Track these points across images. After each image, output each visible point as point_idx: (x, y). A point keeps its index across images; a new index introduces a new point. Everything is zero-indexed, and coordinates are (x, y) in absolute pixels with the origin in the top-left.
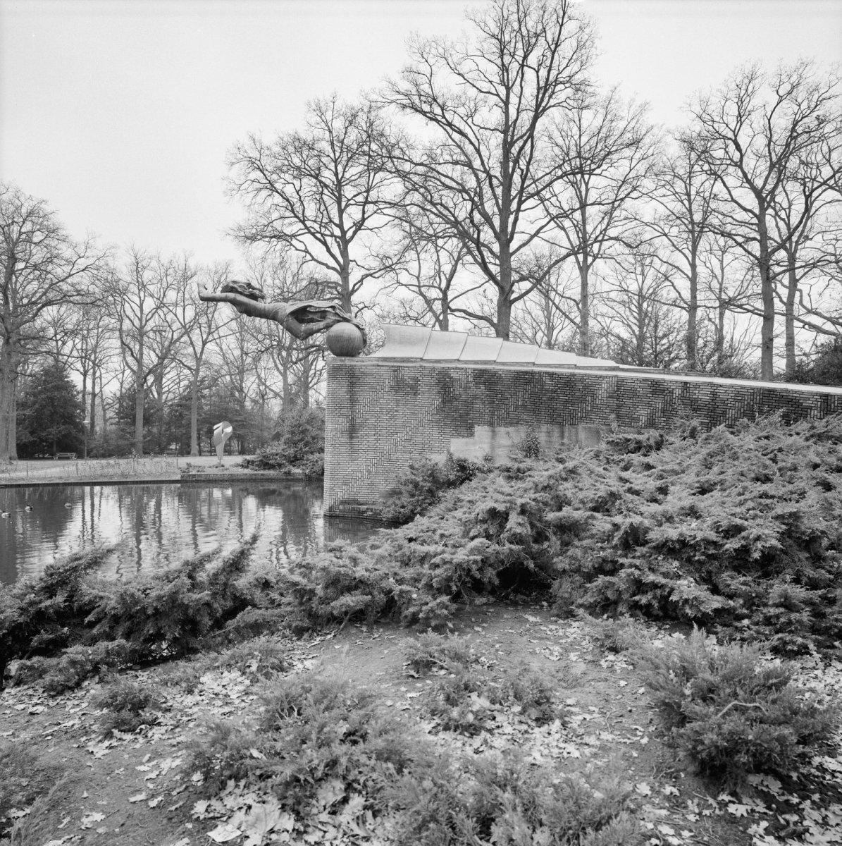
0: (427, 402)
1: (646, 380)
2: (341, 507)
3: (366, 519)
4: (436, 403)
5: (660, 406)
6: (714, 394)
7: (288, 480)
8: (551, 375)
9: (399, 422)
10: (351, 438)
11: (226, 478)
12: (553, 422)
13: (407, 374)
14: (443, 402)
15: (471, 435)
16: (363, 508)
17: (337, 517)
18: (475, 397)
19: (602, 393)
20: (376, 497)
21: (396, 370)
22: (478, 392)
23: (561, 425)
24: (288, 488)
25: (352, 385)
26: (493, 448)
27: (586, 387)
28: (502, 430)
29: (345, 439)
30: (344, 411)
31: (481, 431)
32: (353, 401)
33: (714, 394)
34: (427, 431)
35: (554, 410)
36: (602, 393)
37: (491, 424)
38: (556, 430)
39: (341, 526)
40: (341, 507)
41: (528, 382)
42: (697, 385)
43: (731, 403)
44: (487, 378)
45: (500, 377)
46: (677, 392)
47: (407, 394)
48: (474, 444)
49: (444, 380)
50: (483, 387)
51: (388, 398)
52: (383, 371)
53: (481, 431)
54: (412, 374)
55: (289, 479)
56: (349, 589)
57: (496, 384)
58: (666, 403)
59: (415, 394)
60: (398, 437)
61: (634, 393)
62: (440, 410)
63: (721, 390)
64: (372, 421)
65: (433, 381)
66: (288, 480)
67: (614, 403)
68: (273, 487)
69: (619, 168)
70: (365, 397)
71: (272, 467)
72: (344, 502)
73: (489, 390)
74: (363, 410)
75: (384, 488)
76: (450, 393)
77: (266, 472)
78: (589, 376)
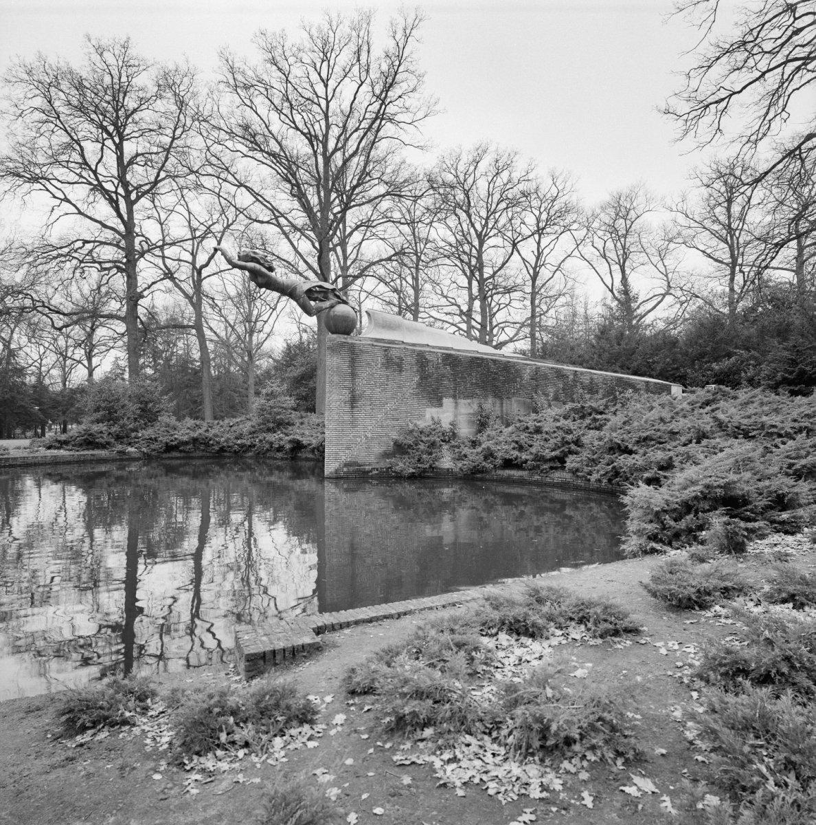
0: (410, 379)
1: (552, 368)
2: (345, 469)
3: (372, 477)
4: (416, 379)
5: (561, 386)
6: (592, 379)
7: (122, 460)
8: (494, 361)
9: (389, 394)
10: (353, 407)
11: (48, 460)
12: (496, 396)
13: (394, 353)
14: (421, 379)
15: (441, 405)
16: (367, 468)
17: (341, 478)
18: (443, 376)
19: (526, 377)
20: (372, 459)
21: (387, 350)
22: (445, 371)
23: (501, 399)
24: (122, 468)
25: (353, 362)
26: (456, 416)
27: (517, 371)
28: (462, 402)
29: (347, 409)
30: (346, 384)
31: (448, 402)
32: (353, 375)
33: (592, 379)
34: (410, 402)
35: (497, 387)
36: (526, 377)
37: (454, 397)
38: (498, 402)
39: (345, 486)
40: (345, 469)
41: (479, 365)
42: (582, 373)
43: (600, 385)
44: (451, 359)
45: (460, 361)
46: (571, 377)
47: (394, 371)
48: (443, 412)
49: (422, 359)
50: (448, 368)
51: (380, 373)
52: (376, 350)
53: (448, 402)
54: (398, 355)
55: (124, 459)
56: (783, 523)
57: (457, 366)
58: (565, 384)
59: (400, 371)
60: (388, 407)
61: (545, 377)
62: (419, 385)
63: (595, 377)
64: (368, 392)
65: (414, 361)
66: (122, 460)
67: (534, 383)
68: (103, 468)
69: (574, 216)
70: (363, 373)
71: (103, 446)
72: (346, 465)
73: (453, 370)
74: (361, 383)
75: (378, 449)
76: (425, 371)
77: (96, 452)
78: (518, 363)
